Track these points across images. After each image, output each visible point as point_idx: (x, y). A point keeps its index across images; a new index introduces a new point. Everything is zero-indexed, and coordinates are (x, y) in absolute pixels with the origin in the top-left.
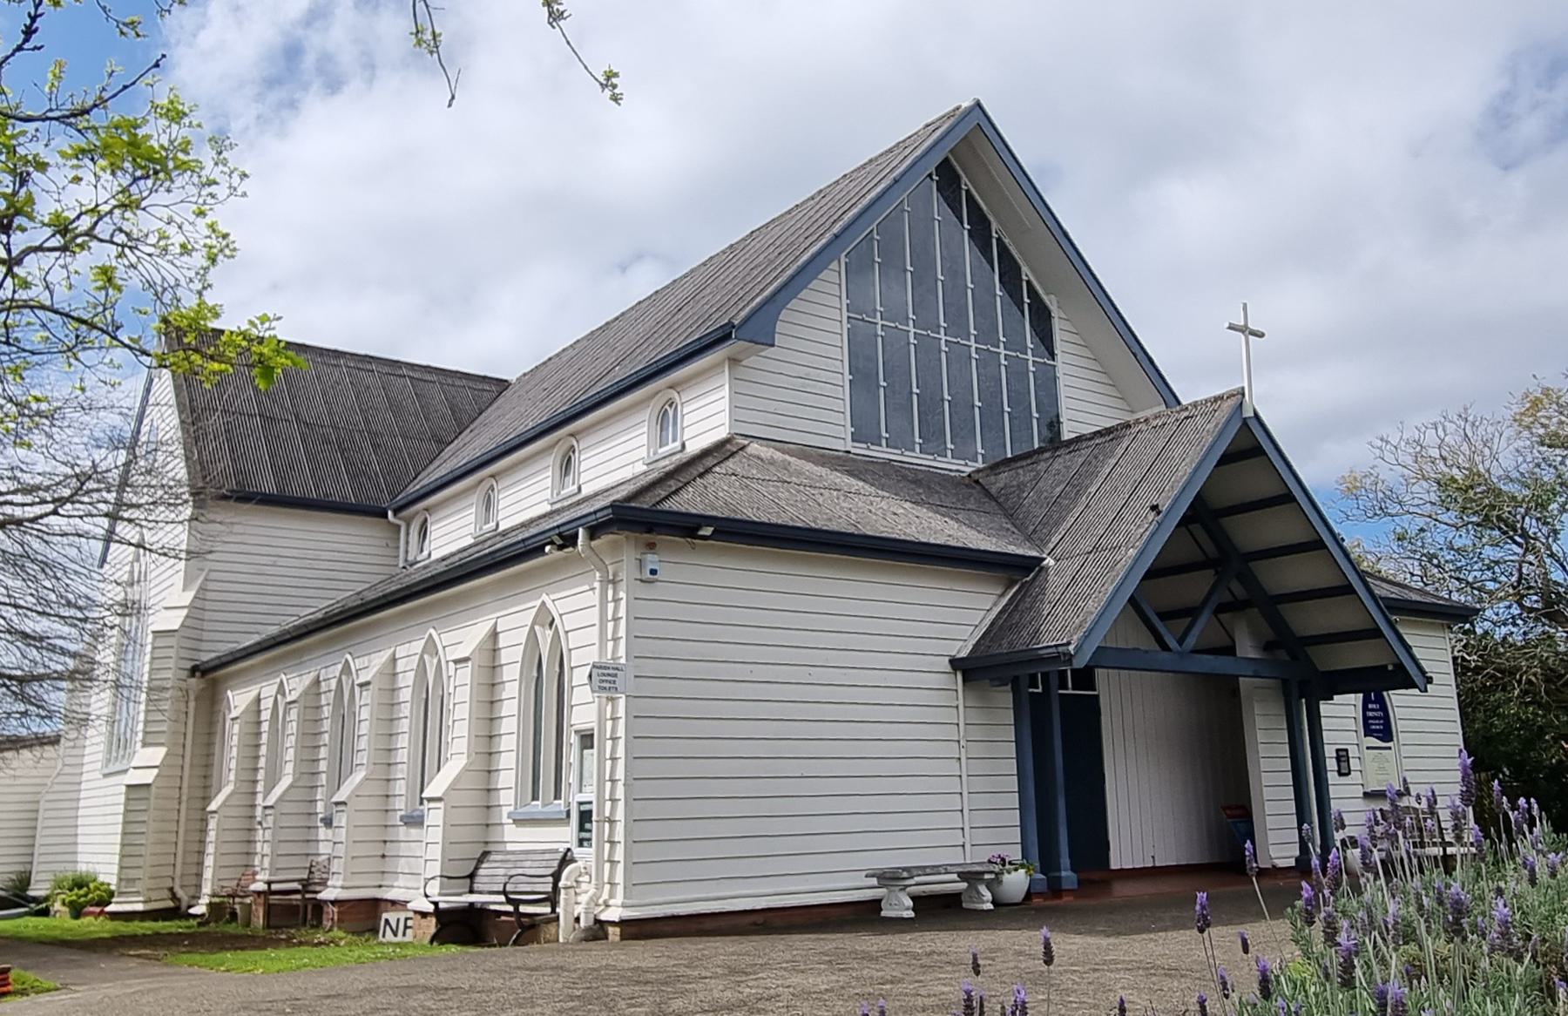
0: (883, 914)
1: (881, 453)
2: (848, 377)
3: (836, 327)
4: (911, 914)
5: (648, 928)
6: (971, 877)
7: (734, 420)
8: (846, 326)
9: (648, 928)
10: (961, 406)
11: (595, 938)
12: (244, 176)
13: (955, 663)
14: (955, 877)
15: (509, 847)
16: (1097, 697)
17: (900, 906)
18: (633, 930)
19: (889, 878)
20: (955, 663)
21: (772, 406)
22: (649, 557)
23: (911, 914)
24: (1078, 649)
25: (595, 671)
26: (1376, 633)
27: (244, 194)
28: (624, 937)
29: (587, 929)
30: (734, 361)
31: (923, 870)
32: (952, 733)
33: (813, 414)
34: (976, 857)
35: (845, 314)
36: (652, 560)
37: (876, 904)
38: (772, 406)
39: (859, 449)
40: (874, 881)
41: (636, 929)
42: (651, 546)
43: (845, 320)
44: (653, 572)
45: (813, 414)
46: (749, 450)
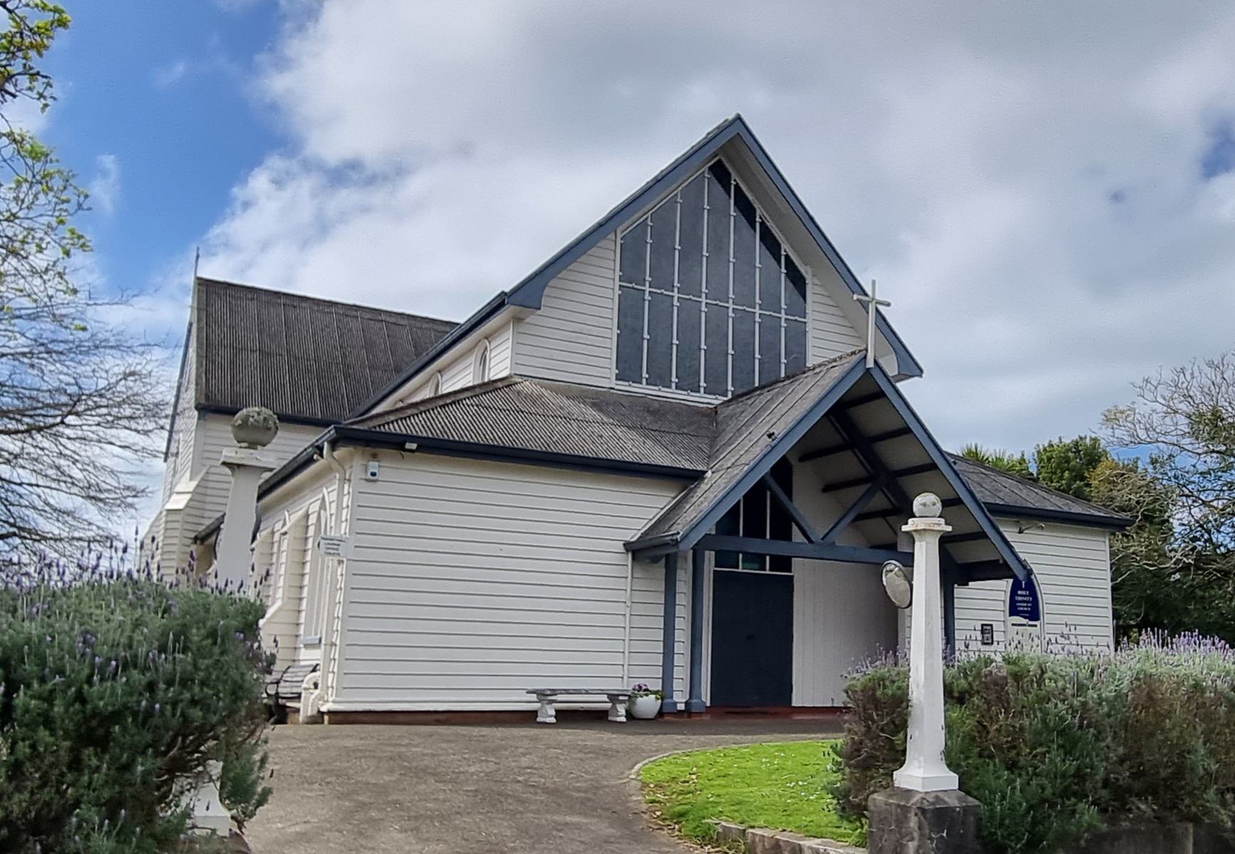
0: (539, 719)
1: (642, 389)
2: (616, 331)
3: (609, 293)
4: (554, 720)
5: (352, 717)
6: (613, 698)
7: (515, 364)
8: (618, 292)
9: (352, 717)
10: (717, 354)
11: (315, 723)
12: (86, 196)
13: (628, 546)
14: (605, 698)
15: (302, 663)
16: (792, 577)
17: (548, 714)
18: (339, 717)
19: (542, 695)
20: (628, 546)
21: (547, 353)
22: (371, 463)
23: (554, 720)
24: (683, 538)
25: (322, 542)
26: (983, 535)
27: (89, 209)
28: (330, 723)
29: (312, 717)
30: (518, 320)
31: (567, 692)
32: (621, 596)
33: (583, 359)
34: (615, 686)
35: (618, 283)
36: (373, 466)
37: (534, 713)
38: (547, 353)
39: (623, 386)
40: (534, 697)
41: (340, 717)
42: (374, 457)
43: (617, 288)
44: (373, 474)
45: (583, 359)
46: (518, 387)
